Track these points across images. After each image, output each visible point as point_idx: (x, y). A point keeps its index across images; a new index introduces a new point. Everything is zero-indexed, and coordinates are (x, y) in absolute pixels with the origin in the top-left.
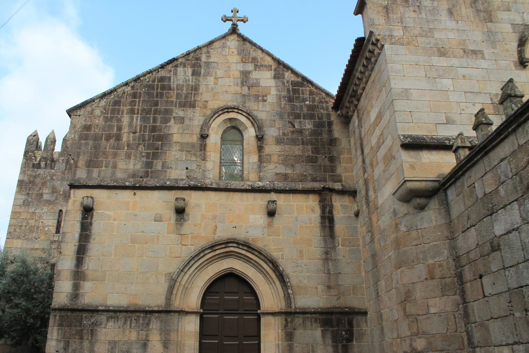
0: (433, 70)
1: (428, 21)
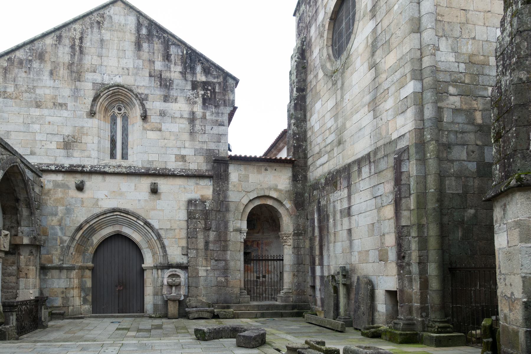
0: (29, 118)
1: (33, 80)
